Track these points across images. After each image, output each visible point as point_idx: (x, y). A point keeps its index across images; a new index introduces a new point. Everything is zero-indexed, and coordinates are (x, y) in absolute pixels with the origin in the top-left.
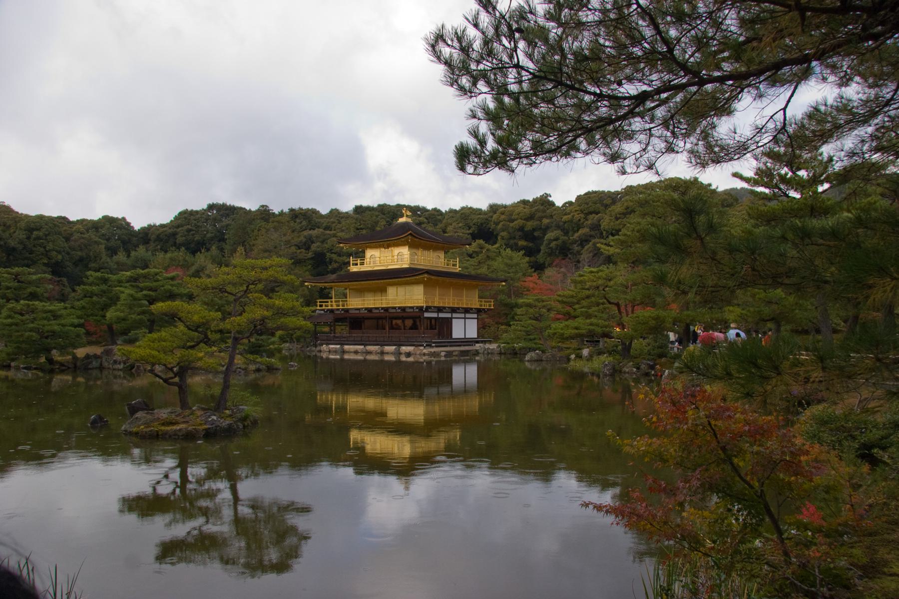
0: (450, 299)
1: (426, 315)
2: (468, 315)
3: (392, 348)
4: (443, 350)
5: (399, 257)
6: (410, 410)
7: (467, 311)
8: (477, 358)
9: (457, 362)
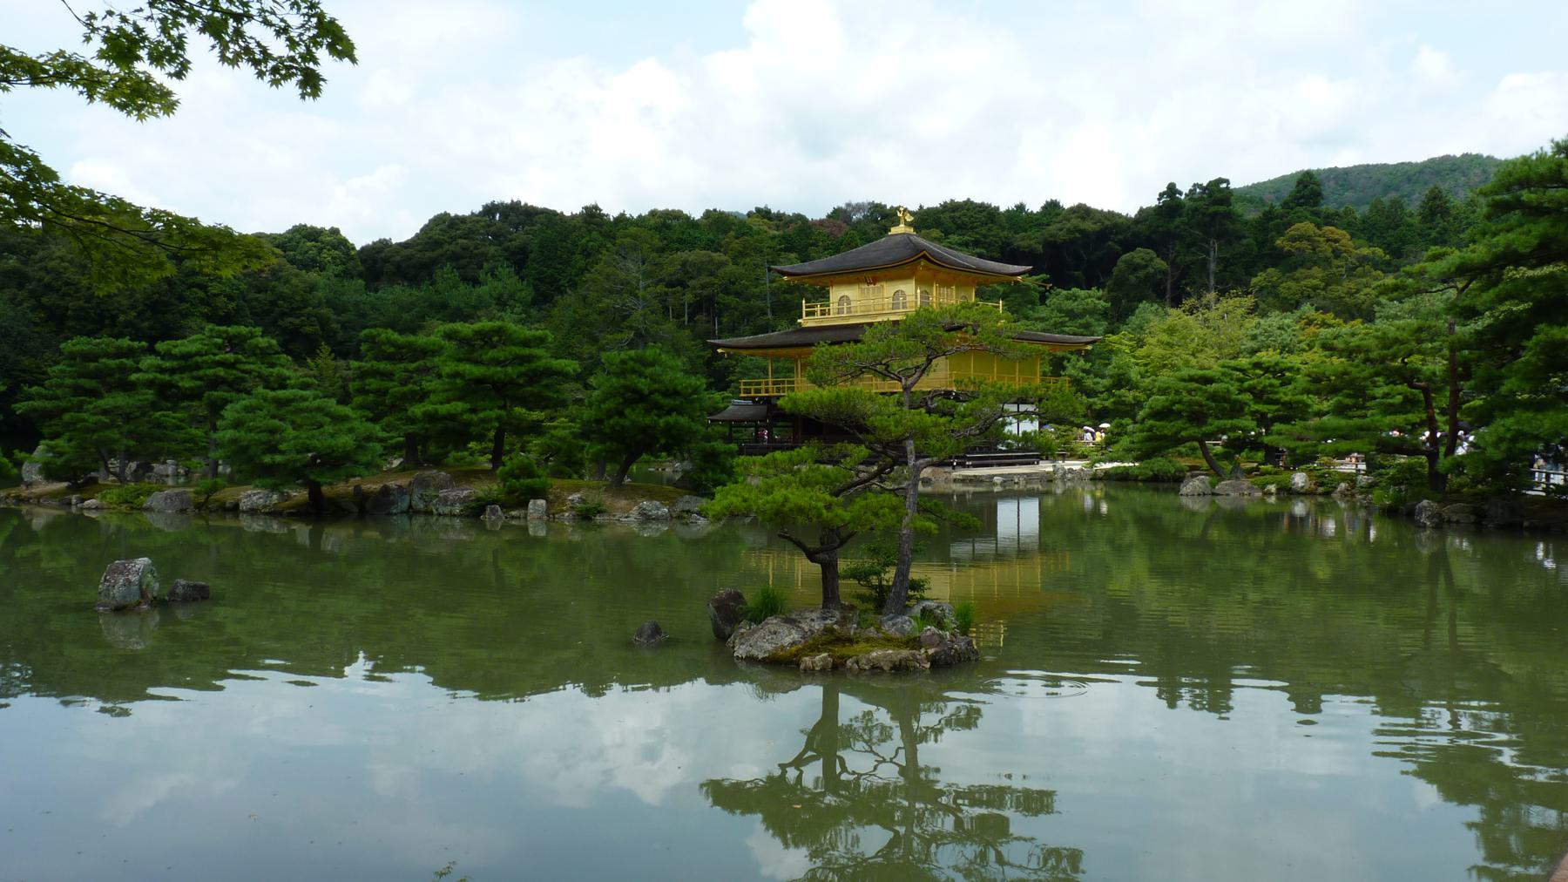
0: (995, 377)
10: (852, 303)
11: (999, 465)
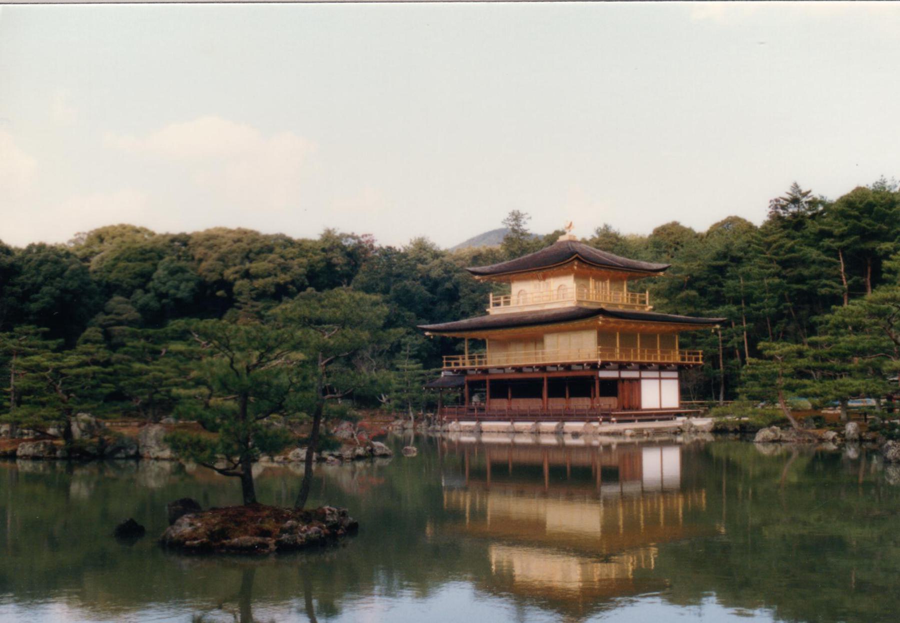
1: (603, 374)
2: (664, 374)
3: (551, 425)
4: (629, 428)
5: (558, 293)
6: (580, 517)
7: (662, 368)
8: (680, 439)
9: (650, 444)
10: (530, 296)
11: (640, 421)
